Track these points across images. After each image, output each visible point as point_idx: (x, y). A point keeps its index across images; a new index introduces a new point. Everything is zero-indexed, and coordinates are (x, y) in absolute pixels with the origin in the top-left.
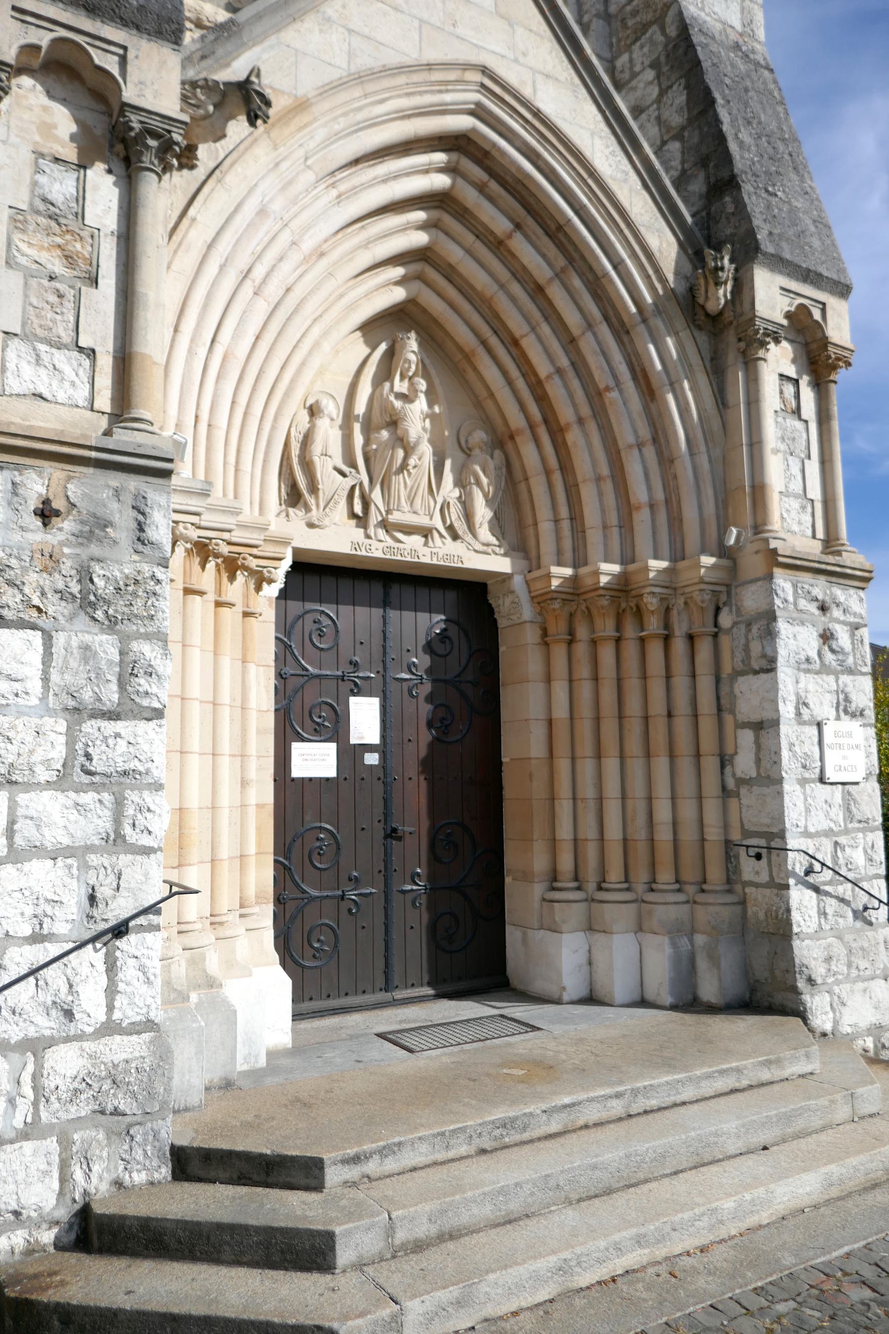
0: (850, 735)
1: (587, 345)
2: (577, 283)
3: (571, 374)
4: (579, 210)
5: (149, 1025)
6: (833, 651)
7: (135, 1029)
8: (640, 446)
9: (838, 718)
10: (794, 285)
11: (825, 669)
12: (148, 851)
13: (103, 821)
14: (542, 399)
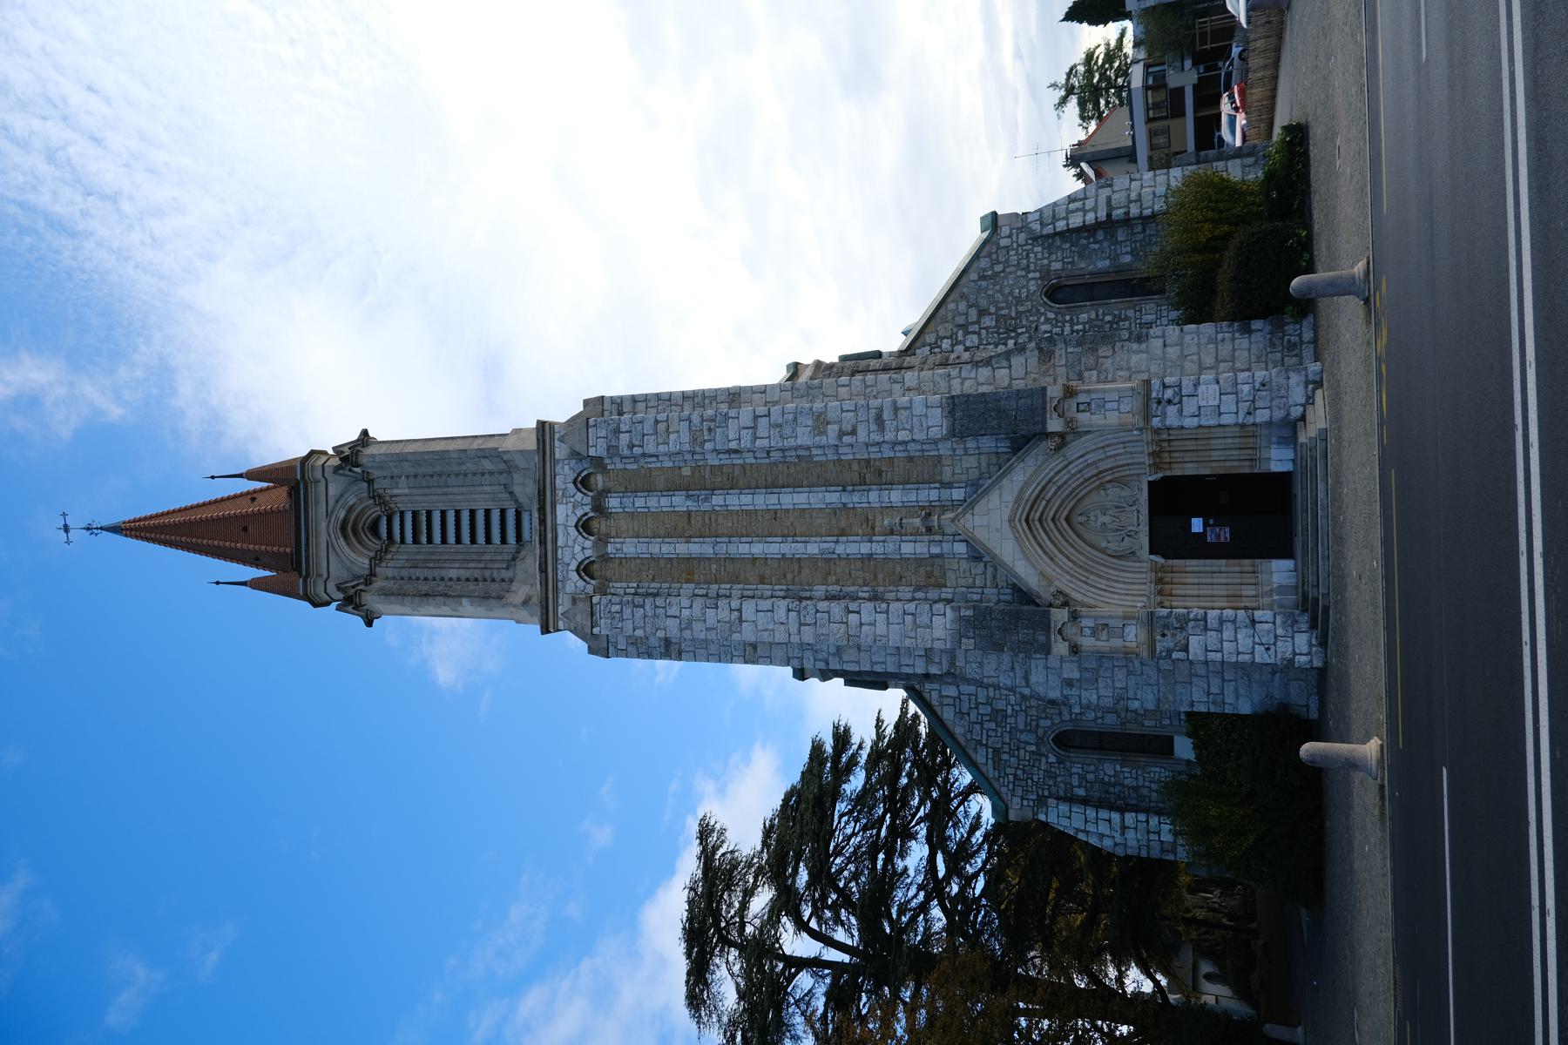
0: (1203, 392)
1: (1073, 472)
2: (1056, 479)
3: (1082, 473)
4: (1038, 485)
5: (1275, 615)
6: (1174, 398)
7: (1275, 618)
8: (1105, 452)
9: (1197, 396)
10: (1048, 416)
11: (1180, 402)
12: (1236, 615)
13: (1229, 624)
14: (1090, 478)
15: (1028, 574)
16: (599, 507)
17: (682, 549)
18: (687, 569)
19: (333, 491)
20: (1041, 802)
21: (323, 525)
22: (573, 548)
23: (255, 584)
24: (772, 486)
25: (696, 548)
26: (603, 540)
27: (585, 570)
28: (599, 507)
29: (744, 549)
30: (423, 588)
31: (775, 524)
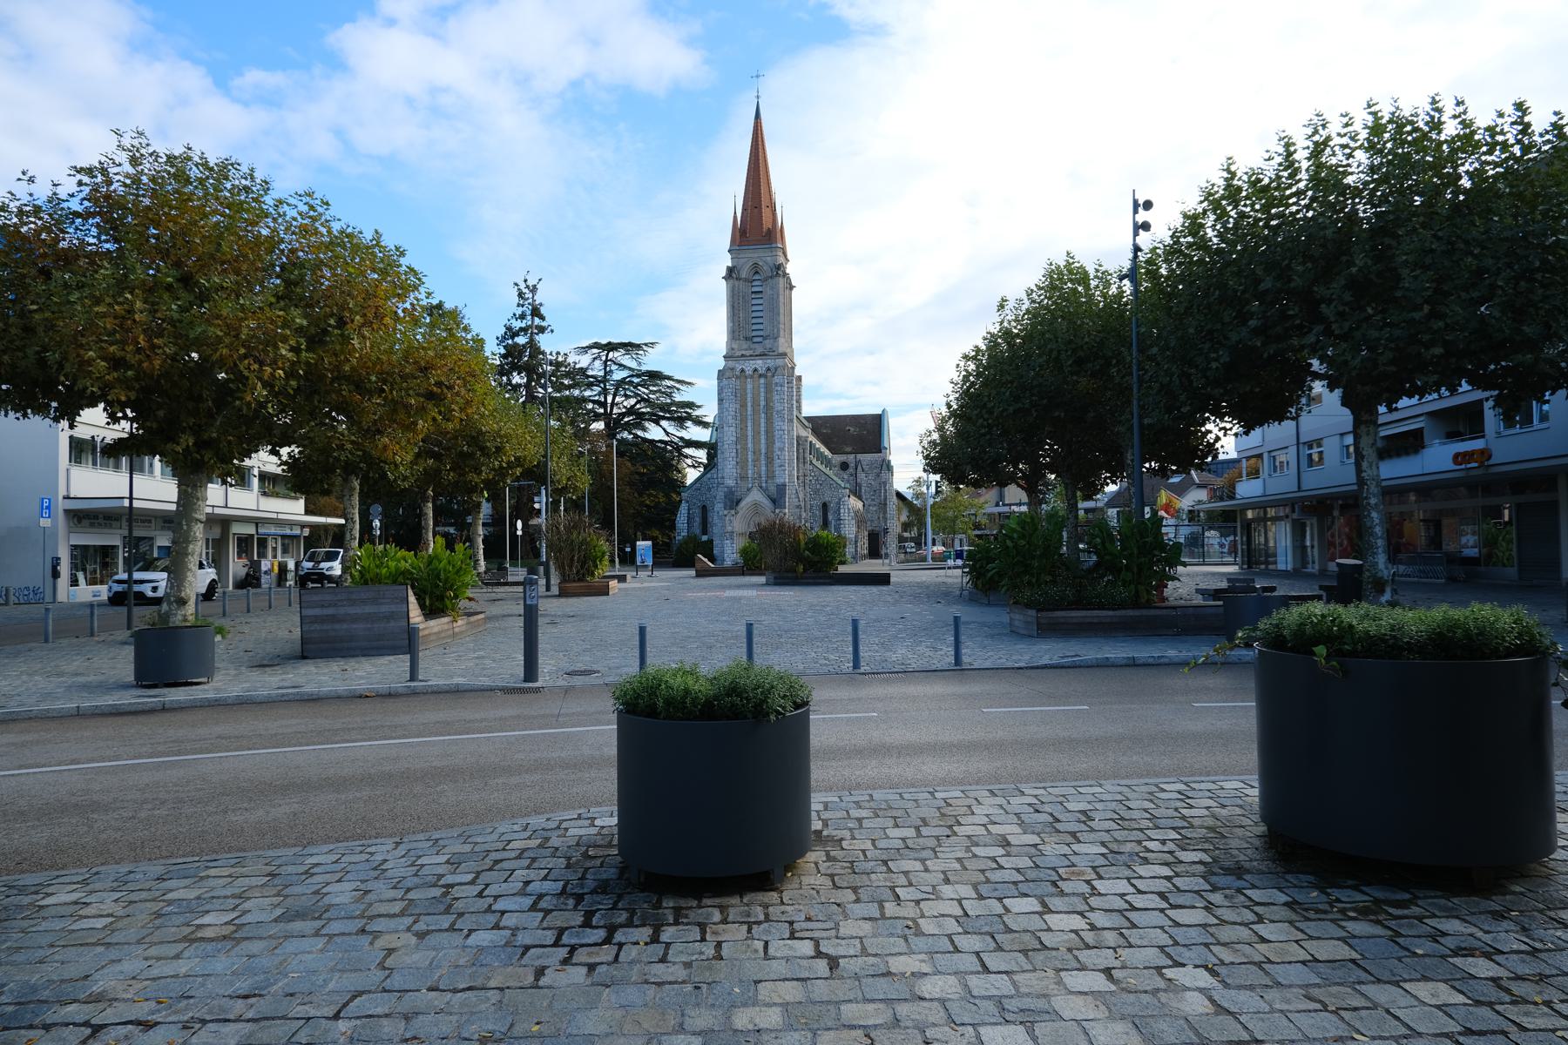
15: (743, 504)
16: (761, 376)
17: (749, 404)
18: (743, 406)
19: (769, 259)
20: (687, 502)
21: (756, 255)
22: (749, 366)
23: (735, 217)
24: (767, 432)
25: (749, 409)
26: (752, 377)
27: (743, 371)
28: (761, 376)
29: (749, 424)
30: (736, 304)
31: (756, 433)
